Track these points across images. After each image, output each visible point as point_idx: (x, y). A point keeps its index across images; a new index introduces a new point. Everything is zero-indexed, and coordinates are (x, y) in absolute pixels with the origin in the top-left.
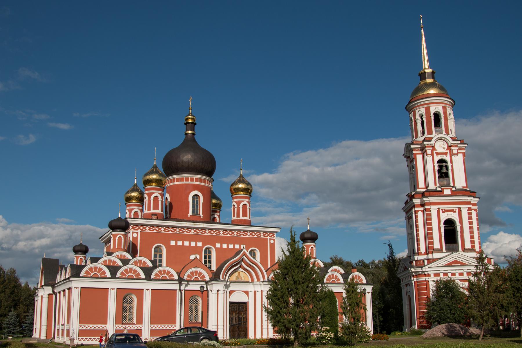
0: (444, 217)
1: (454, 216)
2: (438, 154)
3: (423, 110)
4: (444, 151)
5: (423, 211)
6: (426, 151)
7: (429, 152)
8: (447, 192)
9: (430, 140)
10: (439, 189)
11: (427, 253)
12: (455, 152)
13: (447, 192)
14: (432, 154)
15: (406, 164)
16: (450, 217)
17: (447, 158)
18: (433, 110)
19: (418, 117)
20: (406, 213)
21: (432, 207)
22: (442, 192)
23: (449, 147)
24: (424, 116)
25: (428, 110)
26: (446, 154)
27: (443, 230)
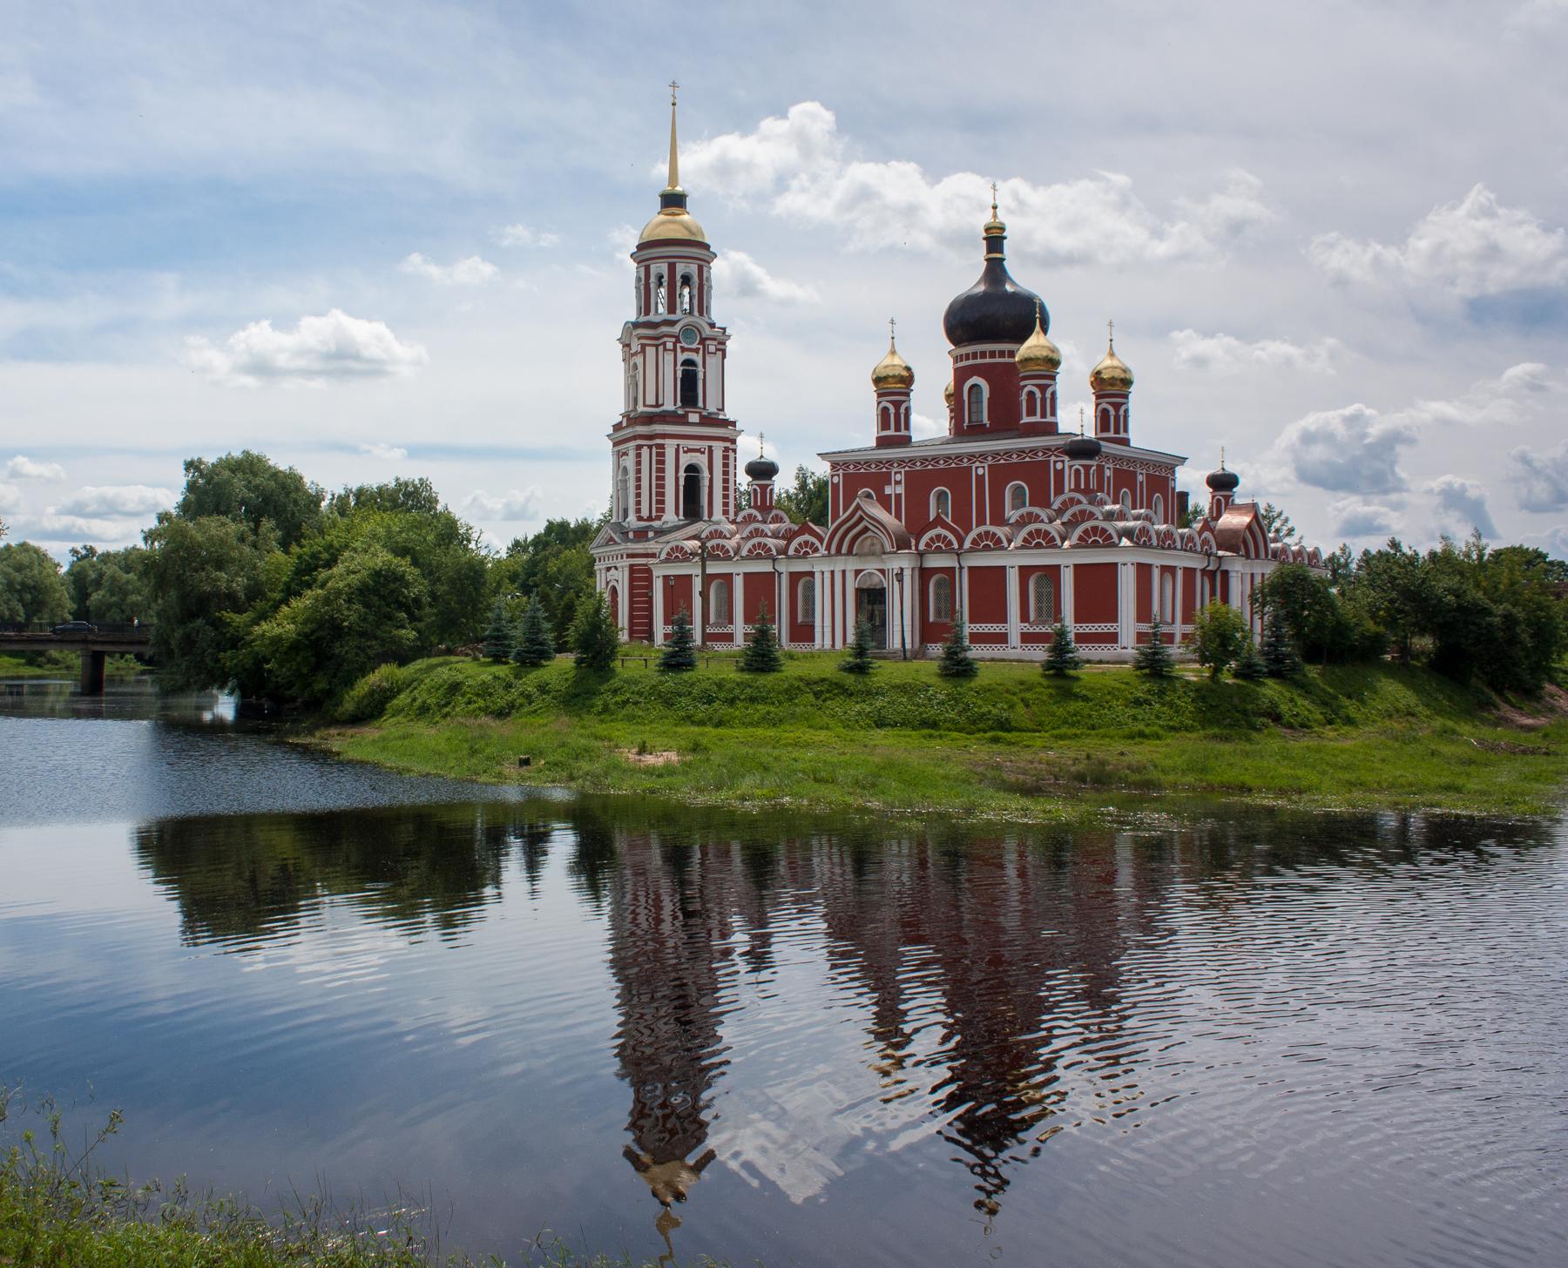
0: (685, 460)
1: (702, 461)
2: (683, 350)
3: (661, 268)
4: (694, 346)
5: (650, 447)
6: (664, 344)
7: (670, 346)
8: (694, 418)
9: (672, 323)
10: (680, 412)
11: (650, 519)
12: (712, 349)
13: (694, 418)
14: (675, 350)
15: (620, 355)
16: (694, 461)
17: (698, 359)
18: (681, 269)
19: (653, 279)
20: (615, 445)
21: (667, 442)
22: (685, 416)
23: (703, 341)
24: (665, 279)
25: (672, 268)
26: (697, 351)
27: (682, 482)
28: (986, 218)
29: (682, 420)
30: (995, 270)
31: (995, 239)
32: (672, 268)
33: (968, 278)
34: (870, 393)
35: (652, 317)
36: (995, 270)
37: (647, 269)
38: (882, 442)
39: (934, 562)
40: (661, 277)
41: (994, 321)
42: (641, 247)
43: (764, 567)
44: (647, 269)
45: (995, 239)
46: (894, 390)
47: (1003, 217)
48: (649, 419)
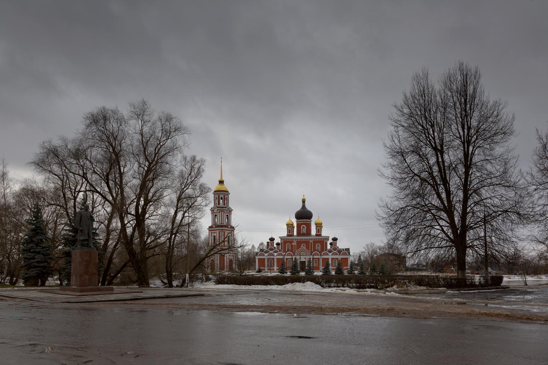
25: (224, 196)
28: (302, 198)
29: (227, 227)
30: (304, 206)
31: (304, 201)
32: (224, 196)
33: (299, 207)
34: (286, 227)
35: (220, 206)
36: (304, 206)
37: (219, 196)
38: (288, 235)
39: (315, 257)
40: (222, 198)
41: (304, 215)
42: (215, 191)
43: (281, 257)
44: (219, 196)
45: (304, 201)
46: (290, 226)
47: (305, 198)
48: (222, 226)
